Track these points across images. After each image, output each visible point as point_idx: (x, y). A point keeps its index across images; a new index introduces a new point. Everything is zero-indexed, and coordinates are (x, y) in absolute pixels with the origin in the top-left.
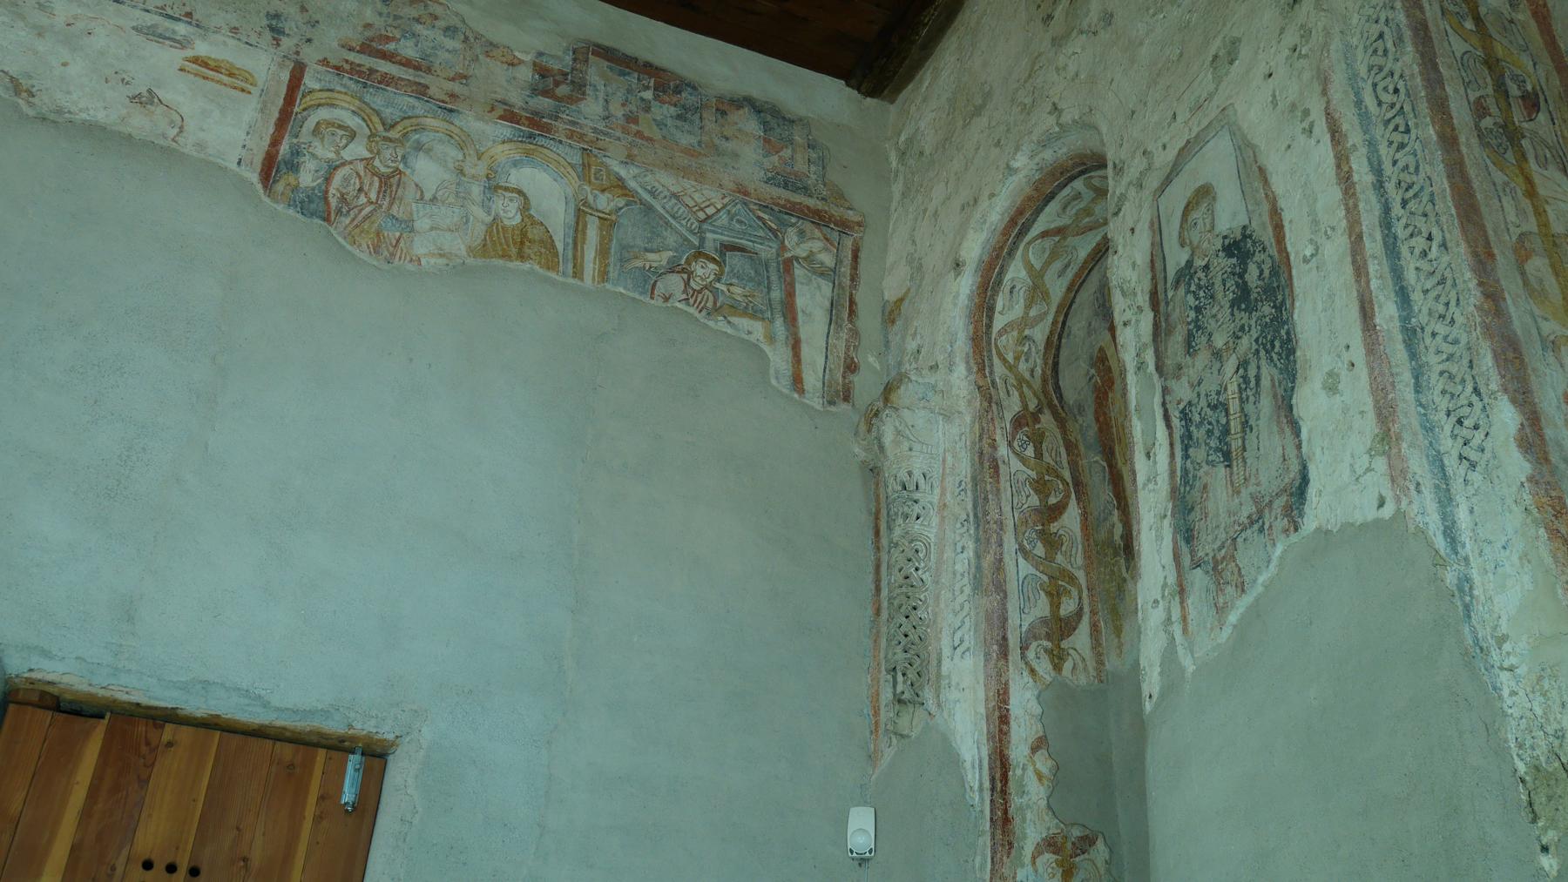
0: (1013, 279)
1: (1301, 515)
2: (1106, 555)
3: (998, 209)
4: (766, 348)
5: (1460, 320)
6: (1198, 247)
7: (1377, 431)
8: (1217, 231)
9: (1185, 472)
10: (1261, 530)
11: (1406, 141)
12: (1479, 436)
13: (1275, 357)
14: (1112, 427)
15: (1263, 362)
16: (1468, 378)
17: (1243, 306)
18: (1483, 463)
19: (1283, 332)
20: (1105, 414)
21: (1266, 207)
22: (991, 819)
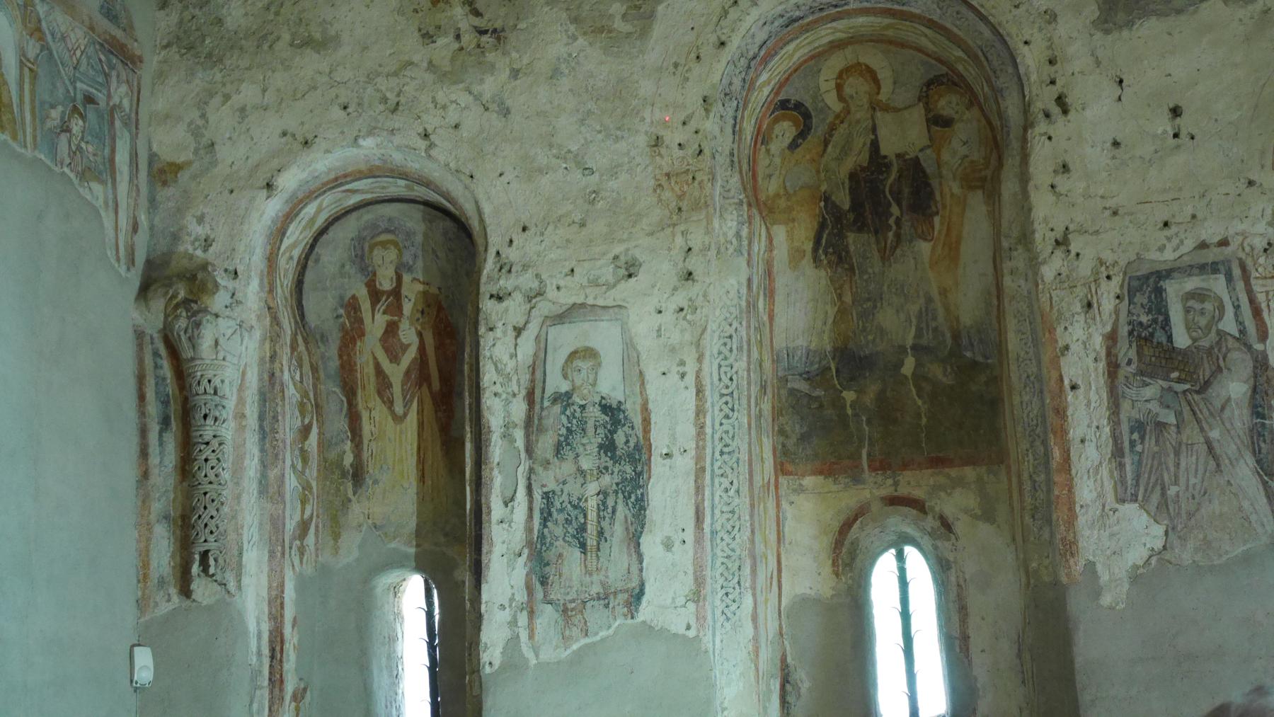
1: (637, 610)
3: (326, 162)
4: (103, 214)
5: (738, 540)
6: (579, 388)
7: (693, 588)
9: (542, 537)
10: (607, 606)
11: (731, 415)
13: (630, 505)
14: (357, 371)
15: (620, 501)
16: (737, 574)
17: (609, 454)
18: (733, 620)
19: (639, 492)
20: (349, 355)
21: (639, 400)
22: (270, 679)
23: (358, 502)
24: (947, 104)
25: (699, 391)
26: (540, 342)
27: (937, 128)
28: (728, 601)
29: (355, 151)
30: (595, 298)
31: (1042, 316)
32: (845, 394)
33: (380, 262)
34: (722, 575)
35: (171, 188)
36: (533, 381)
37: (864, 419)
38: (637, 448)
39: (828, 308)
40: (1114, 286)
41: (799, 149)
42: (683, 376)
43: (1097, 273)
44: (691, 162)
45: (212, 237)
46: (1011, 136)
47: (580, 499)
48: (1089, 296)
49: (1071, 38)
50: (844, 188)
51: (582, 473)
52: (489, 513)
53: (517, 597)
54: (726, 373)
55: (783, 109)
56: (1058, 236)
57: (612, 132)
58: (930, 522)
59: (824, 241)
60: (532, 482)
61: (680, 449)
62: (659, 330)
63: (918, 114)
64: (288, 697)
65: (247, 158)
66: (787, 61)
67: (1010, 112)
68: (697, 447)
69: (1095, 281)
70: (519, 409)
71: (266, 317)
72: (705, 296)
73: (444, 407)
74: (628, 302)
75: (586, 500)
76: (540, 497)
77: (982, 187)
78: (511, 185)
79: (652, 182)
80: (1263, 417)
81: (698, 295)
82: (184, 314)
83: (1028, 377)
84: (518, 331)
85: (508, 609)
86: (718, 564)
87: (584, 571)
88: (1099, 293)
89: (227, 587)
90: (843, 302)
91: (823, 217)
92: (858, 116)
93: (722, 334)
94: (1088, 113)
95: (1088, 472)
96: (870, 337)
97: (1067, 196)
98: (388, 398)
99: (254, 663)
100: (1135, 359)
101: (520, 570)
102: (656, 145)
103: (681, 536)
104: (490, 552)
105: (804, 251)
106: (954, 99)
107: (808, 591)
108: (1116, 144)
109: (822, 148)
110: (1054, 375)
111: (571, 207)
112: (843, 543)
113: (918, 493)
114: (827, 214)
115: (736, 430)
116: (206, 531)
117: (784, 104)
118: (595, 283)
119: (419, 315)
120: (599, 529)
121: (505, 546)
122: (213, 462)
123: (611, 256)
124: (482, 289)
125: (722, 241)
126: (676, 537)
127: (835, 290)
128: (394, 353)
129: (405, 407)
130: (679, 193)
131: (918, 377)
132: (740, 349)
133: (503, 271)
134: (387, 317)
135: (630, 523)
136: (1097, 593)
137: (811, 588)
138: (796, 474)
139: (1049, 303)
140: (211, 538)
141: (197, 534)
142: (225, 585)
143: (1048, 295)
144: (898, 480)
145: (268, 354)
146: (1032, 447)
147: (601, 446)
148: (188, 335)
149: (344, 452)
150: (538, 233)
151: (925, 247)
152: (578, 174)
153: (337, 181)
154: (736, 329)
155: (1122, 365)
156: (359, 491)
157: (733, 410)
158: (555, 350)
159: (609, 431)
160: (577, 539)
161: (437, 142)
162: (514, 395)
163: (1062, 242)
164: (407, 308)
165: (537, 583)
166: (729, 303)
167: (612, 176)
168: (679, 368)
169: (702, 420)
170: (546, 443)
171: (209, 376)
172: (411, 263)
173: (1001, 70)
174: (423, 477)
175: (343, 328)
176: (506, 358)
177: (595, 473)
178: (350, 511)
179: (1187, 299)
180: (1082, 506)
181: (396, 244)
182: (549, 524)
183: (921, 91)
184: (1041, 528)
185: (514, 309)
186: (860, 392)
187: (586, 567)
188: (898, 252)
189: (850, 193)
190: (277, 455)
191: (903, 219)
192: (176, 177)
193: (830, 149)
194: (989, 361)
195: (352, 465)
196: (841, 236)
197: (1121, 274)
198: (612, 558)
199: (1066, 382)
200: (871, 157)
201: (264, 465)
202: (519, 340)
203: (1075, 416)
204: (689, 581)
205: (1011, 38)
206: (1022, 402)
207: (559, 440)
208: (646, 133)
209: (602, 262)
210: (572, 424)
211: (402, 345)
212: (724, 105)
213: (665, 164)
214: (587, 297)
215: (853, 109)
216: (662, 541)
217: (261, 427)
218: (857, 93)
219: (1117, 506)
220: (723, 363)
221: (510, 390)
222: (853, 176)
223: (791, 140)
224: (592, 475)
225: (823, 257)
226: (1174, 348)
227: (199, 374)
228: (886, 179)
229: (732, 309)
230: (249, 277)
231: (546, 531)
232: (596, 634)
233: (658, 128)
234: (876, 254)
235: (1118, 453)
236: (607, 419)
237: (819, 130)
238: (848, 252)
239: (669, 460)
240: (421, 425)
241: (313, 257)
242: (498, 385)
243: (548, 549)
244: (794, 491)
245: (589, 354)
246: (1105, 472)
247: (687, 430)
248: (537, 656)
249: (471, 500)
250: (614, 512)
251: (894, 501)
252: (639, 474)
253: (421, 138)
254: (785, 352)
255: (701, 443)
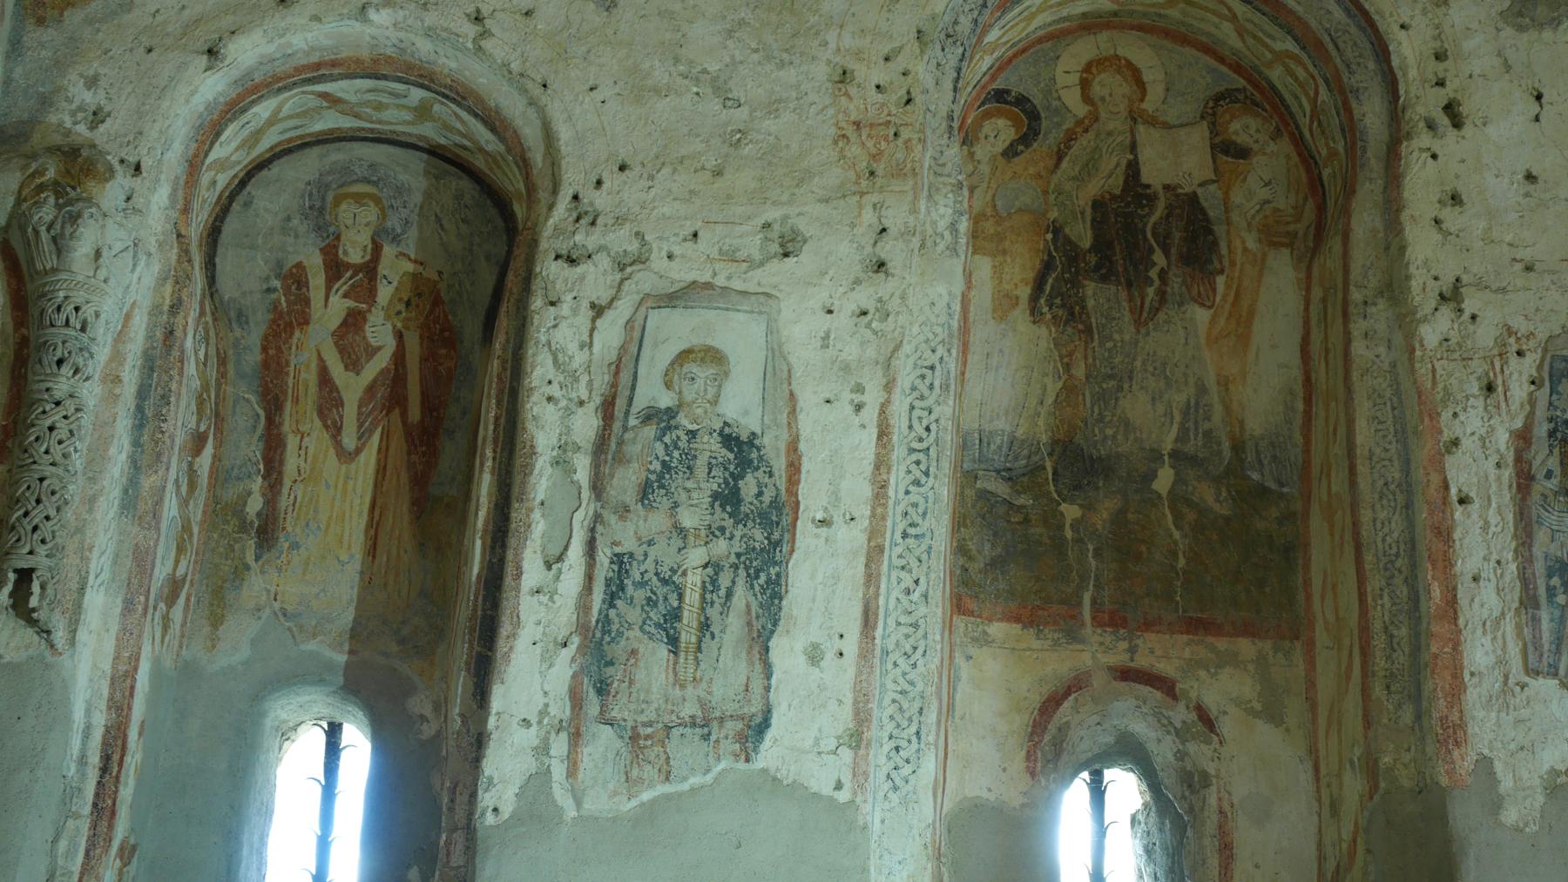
0: (255, 114)
1: (756, 750)
2: (227, 522)
3: (309, 36)
5: (921, 668)
7: (851, 726)
8: (720, 410)
9: (605, 621)
10: (706, 737)
11: (923, 482)
12: (907, 770)
13: (757, 588)
14: (287, 374)
18: (904, 791)
19: (773, 571)
20: (279, 349)
21: (785, 436)
22: (95, 805)
23: (262, 572)
24: (1243, 128)
25: (883, 433)
26: (632, 328)
27: (1225, 158)
28: (898, 759)
29: (358, 26)
30: (729, 278)
31: (1420, 394)
32: (1064, 507)
33: (349, 222)
34: (892, 717)
35: (49, 30)
36: (614, 385)
37: (1091, 547)
38: (775, 504)
39: (1048, 381)
40: (1529, 365)
41: (1016, 160)
42: (859, 408)
43: (1504, 345)
44: (894, 112)
45: (107, 109)
46: (1369, 154)
47: (673, 571)
48: (1491, 374)
49: (1468, 29)
50: (1084, 222)
51: (681, 531)
52: (519, 576)
53: (553, 710)
54: (920, 418)
55: (998, 102)
56: (1444, 289)
57: (776, 53)
58: (1181, 714)
59: (1048, 288)
60: (597, 536)
61: (844, 515)
62: (827, 336)
63: (1198, 137)
64: (116, 844)
65: (184, 7)
66: (1022, 25)
67: (1368, 121)
68: (873, 515)
69: (1500, 355)
70: (586, 425)
71: (172, 247)
72: (903, 297)
73: (424, 449)
74: (780, 291)
75: (684, 574)
76: (606, 562)
77: (1291, 245)
78: (607, 106)
79: (833, 131)
81: (893, 294)
82: (52, 200)
83: (1386, 484)
84: (598, 310)
85: (534, 729)
86: (887, 701)
87: (671, 679)
88: (1507, 372)
89: (52, 637)
90: (1071, 376)
91: (1050, 254)
92: (1111, 126)
93: (919, 362)
94: (1491, 130)
95: (1484, 624)
96: (1109, 432)
97: (1458, 236)
98: (334, 423)
99: (70, 774)
100: (1557, 471)
101: (563, 668)
102: (841, 82)
103: (838, 644)
104: (513, 636)
105: (1017, 298)
106: (1254, 123)
107: (985, 794)
108: (1530, 177)
109: (1053, 161)
110: (1435, 479)
111: (700, 147)
112: (1046, 728)
113: (1165, 668)
114: (1056, 250)
115: (930, 505)
116: (35, 536)
117: (1000, 96)
118: (731, 257)
119: (402, 307)
120: (702, 619)
121: (541, 628)
122: (62, 433)
123: (760, 221)
124: (544, 244)
125: (930, 231)
126: (828, 644)
127: (1061, 357)
128: (354, 357)
129: (359, 439)
130: (874, 151)
131: (1178, 499)
132: (945, 387)
133: (582, 222)
134: (351, 303)
135: (754, 615)
136: (1496, 805)
137: (990, 790)
138: (980, 616)
139: (1430, 376)
140: (42, 550)
141: (18, 540)
142: (48, 632)
143: (1430, 366)
144: (1136, 646)
145: (168, 302)
146: (1389, 585)
147: (715, 496)
148: (53, 232)
149: (250, 494)
150: (645, 175)
151: (1201, 315)
152: (715, 105)
153: (317, 71)
154: (942, 358)
155: (1538, 476)
156: (265, 557)
157: (927, 474)
158: (655, 345)
159: (732, 474)
160: (665, 630)
161: (494, 31)
162: (581, 403)
163: (1452, 296)
164: (384, 293)
165: (591, 690)
166: (933, 319)
167: (770, 113)
168: (854, 396)
169: (885, 477)
170: (626, 482)
171: (79, 301)
172: (399, 231)
173: (1359, 64)
174: (375, 548)
175: (275, 308)
176: (573, 348)
177: (703, 533)
178: (246, 584)
180: (1472, 674)
181: (377, 201)
182: (619, 603)
183: (1205, 107)
184: (1399, 705)
185: (595, 279)
186: (1088, 507)
187: (676, 674)
188: (1161, 316)
189: (1093, 227)
190: (159, 455)
191: (1171, 273)
192: (61, 15)
193: (1064, 164)
194: (1285, 490)
195: (259, 514)
196: (1075, 283)
197: (1539, 350)
198: (721, 664)
199: (1453, 491)
200: (1126, 182)
201: (134, 463)
202: (599, 322)
203: (1466, 541)
204: (846, 715)
205: (1383, 17)
206: (1375, 520)
207: (647, 478)
208: (829, 62)
209: (744, 228)
210: (672, 457)
211: (368, 345)
212: (943, 50)
213: (854, 109)
214: (715, 274)
215: (1103, 115)
216: (806, 649)
217: (140, 409)
218: (1111, 95)
219: (1527, 679)
220: (917, 403)
221: (574, 395)
222: (1097, 205)
223: (1007, 143)
224: (697, 536)
225: (1045, 309)
227: (62, 294)
228: (1149, 215)
229: (939, 330)
230: (158, 180)
231: (612, 613)
232: (685, 779)
233: (848, 58)
234: (1127, 316)
235: (1529, 602)
236: (731, 456)
237: (1051, 137)
238: (1083, 308)
239: (825, 529)
240: (381, 469)
241: (241, 199)
242: (555, 386)
243: (613, 640)
244: (974, 640)
245: (713, 356)
246: (1509, 627)
247: (858, 489)
248: (579, 804)
249: (482, 562)
250: (729, 594)
251: (1126, 674)
252: (778, 543)
253: (469, 20)
254: (976, 435)
255: (879, 510)
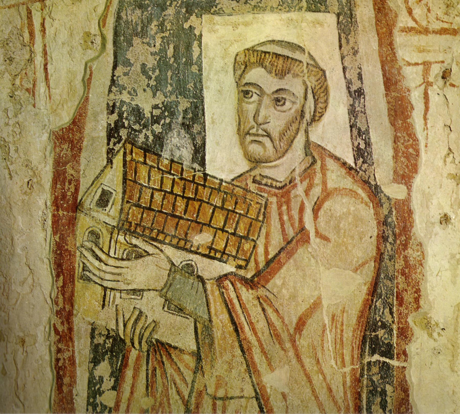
80: (388, 353)
88: (50, 31)
100: (117, 196)
179: (247, 66)
226: (206, 175)
